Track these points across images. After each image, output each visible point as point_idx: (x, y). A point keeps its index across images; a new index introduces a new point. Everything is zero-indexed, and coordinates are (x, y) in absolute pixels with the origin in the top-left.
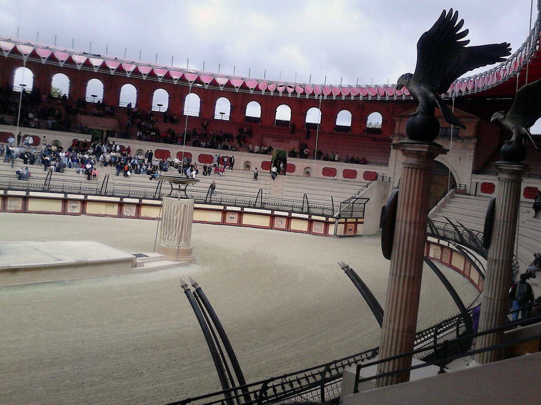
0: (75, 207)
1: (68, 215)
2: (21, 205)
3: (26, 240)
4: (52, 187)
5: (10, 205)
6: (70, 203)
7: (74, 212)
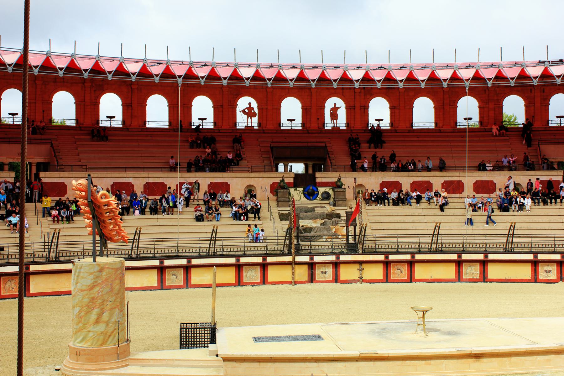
0: (550, 271)
1: (540, 283)
2: (479, 273)
3: (488, 316)
4: (516, 246)
5: (466, 273)
6: (541, 265)
7: (548, 278)
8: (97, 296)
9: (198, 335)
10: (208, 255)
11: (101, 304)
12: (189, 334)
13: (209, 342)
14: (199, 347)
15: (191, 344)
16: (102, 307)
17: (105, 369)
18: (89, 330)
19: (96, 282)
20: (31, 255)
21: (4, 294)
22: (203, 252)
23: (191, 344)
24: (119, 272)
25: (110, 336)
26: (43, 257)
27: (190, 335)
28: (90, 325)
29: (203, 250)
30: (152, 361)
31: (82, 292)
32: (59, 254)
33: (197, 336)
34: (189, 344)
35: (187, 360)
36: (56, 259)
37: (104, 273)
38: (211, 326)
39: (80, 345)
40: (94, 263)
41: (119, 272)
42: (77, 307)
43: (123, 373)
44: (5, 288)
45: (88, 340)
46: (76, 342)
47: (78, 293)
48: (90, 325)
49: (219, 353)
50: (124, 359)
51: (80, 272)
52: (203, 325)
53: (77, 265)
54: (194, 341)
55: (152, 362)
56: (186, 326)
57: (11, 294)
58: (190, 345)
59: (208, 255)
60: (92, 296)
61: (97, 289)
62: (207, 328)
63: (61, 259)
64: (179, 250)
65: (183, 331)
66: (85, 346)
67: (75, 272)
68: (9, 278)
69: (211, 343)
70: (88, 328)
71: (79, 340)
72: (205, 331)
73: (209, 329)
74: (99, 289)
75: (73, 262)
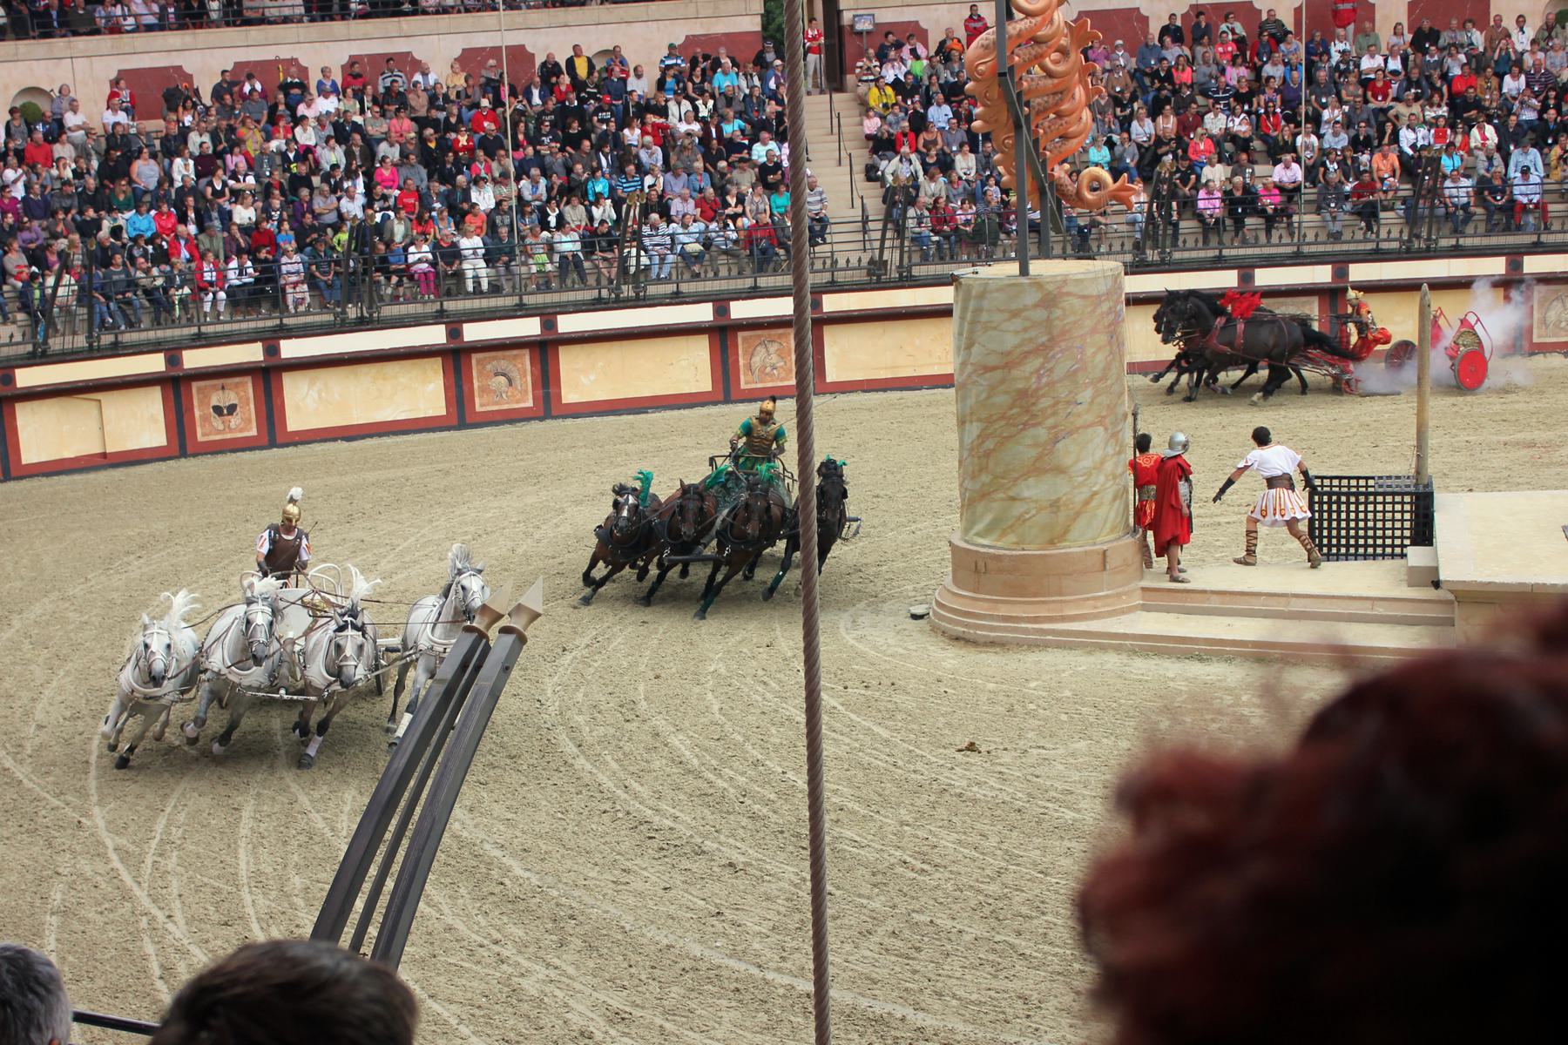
8: (1034, 387)
9: (1370, 516)
10: (1408, 250)
11: (1049, 411)
12: (1339, 512)
13: (1407, 542)
14: (1375, 556)
15: (1348, 546)
16: (1050, 421)
17: (1063, 619)
18: (1011, 493)
19: (1031, 340)
20: (824, 263)
21: (749, 386)
22: (1388, 240)
23: (1348, 546)
24: (1105, 307)
25: (1078, 514)
26: (859, 268)
27: (1343, 516)
28: (1017, 479)
29: (1389, 232)
30: (1215, 597)
31: (987, 375)
32: (910, 258)
33: (1366, 520)
34: (1338, 546)
35: (1333, 597)
36: (901, 274)
37: (1058, 313)
38: (1416, 485)
39: (985, 542)
40: (1024, 280)
41: (1105, 307)
42: (971, 422)
43: (1122, 631)
44: (749, 367)
45: (1011, 527)
46: (973, 532)
47: (974, 378)
48: (1017, 479)
49: (1442, 578)
50: (1126, 589)
51: (978, 311)
52: (1389, 482)
53: (969, 288)
54: (1357, 537)
55: (1215, 602)
56: (1331, 486)
57: (770, 385)
58: (1343, 550)
59: (1408, 250)
60: (1020, 386)
61: (1035, 363)
62: (1402, 494)
63: (916, 271)
64: (1305, 236)
65: (1321, 503)
66: (999, 544)
67: (964, 309)
68: (760, 336)
69: (1414, 543)
70: (1009, 489)
71: (979, 527)
72: (1393, 503)
73: (1407, 499)
74: (1043, 364)
75: (952, 280)
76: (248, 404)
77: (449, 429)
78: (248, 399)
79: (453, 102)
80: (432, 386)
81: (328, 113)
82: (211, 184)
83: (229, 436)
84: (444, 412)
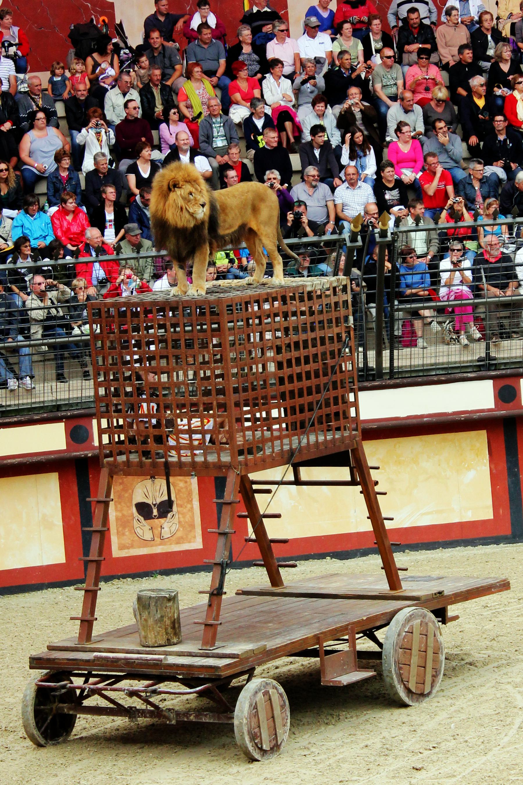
76: (190, 501)
77: (497, 541)
78: (190, 493)
79: (505, 40)
80: (471, 475)
81: (318, 61)
82: (134, 169)
83: (159, 549)
84: (489, 515)
